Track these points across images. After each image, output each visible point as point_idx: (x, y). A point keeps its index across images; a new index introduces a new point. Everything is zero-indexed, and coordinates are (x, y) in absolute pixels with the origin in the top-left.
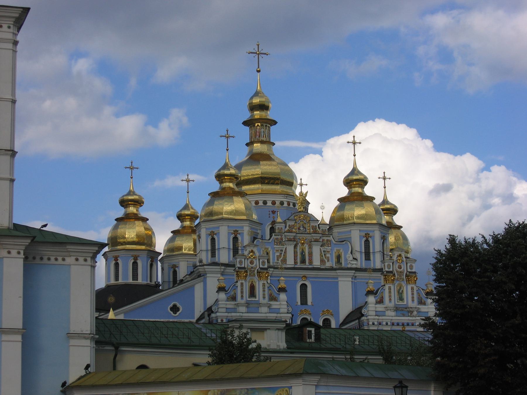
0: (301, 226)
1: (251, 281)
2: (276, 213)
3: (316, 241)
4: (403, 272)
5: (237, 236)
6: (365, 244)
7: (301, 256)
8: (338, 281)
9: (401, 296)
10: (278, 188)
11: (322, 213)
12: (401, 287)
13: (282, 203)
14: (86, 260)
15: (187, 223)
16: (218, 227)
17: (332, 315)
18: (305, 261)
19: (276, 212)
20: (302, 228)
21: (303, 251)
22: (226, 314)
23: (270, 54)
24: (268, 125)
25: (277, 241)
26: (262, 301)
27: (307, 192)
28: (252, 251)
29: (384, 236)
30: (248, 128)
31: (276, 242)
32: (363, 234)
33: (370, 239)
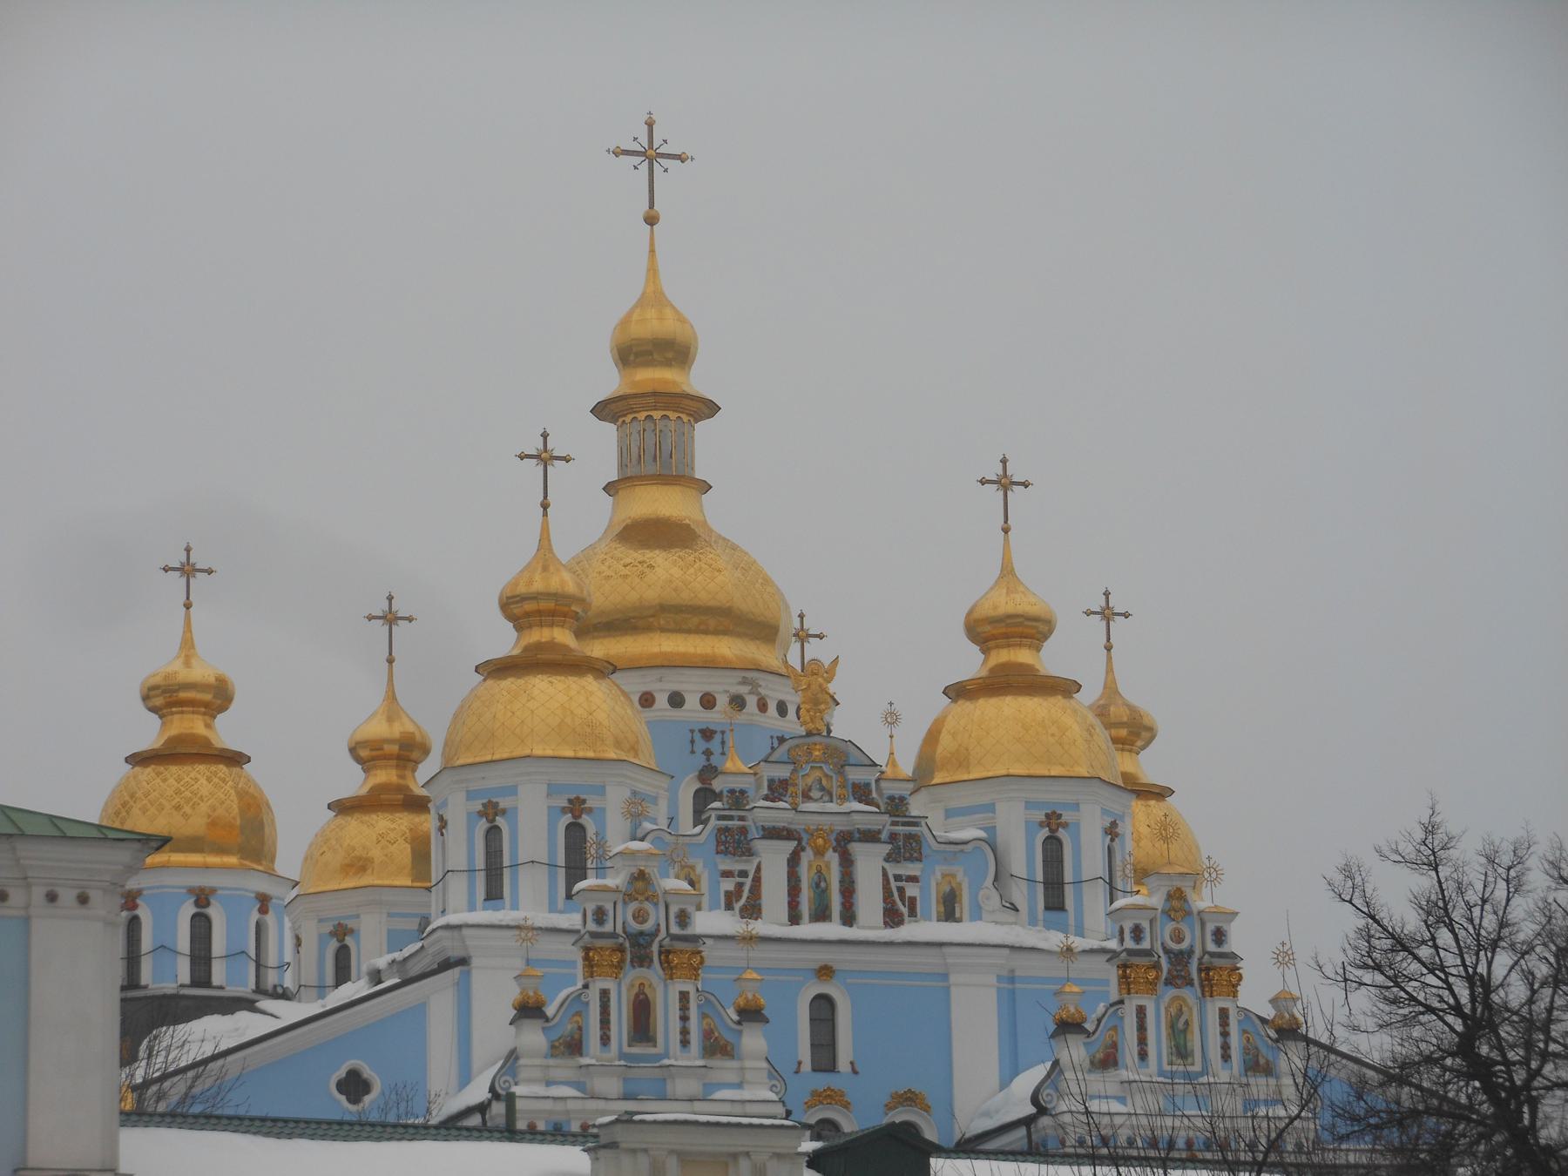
0: (813, 787)
1: (637, 983)
2: (718, 737)
3: (870, 837)
4: (1190, 952)
5: (580, 821)
6: (1044, 850)
7: (812, 895)
8: (947, 990)
9: (1182, 1042)
10: (726, 648)
11: (891, 737)
12: (1181, 1010)
13: (738, 702)
14: (83, 900)
15: (386, 775)
16: (512, 791)
17: (927, 1109)
18: (827, 913)
19: (715, 732)
20: (815, 794)
21: (819, 876)
22: (548, 1105)
23: (692, 159)
24: (685, 418)
25: (726, 837)
26: (679, 1059)
27: (836, 661)
28: (641, 876)
29: (1114, 824)
30: (610, 429)
31: (724, 843)
32: (1040, 816)
33: (1062, 833)
